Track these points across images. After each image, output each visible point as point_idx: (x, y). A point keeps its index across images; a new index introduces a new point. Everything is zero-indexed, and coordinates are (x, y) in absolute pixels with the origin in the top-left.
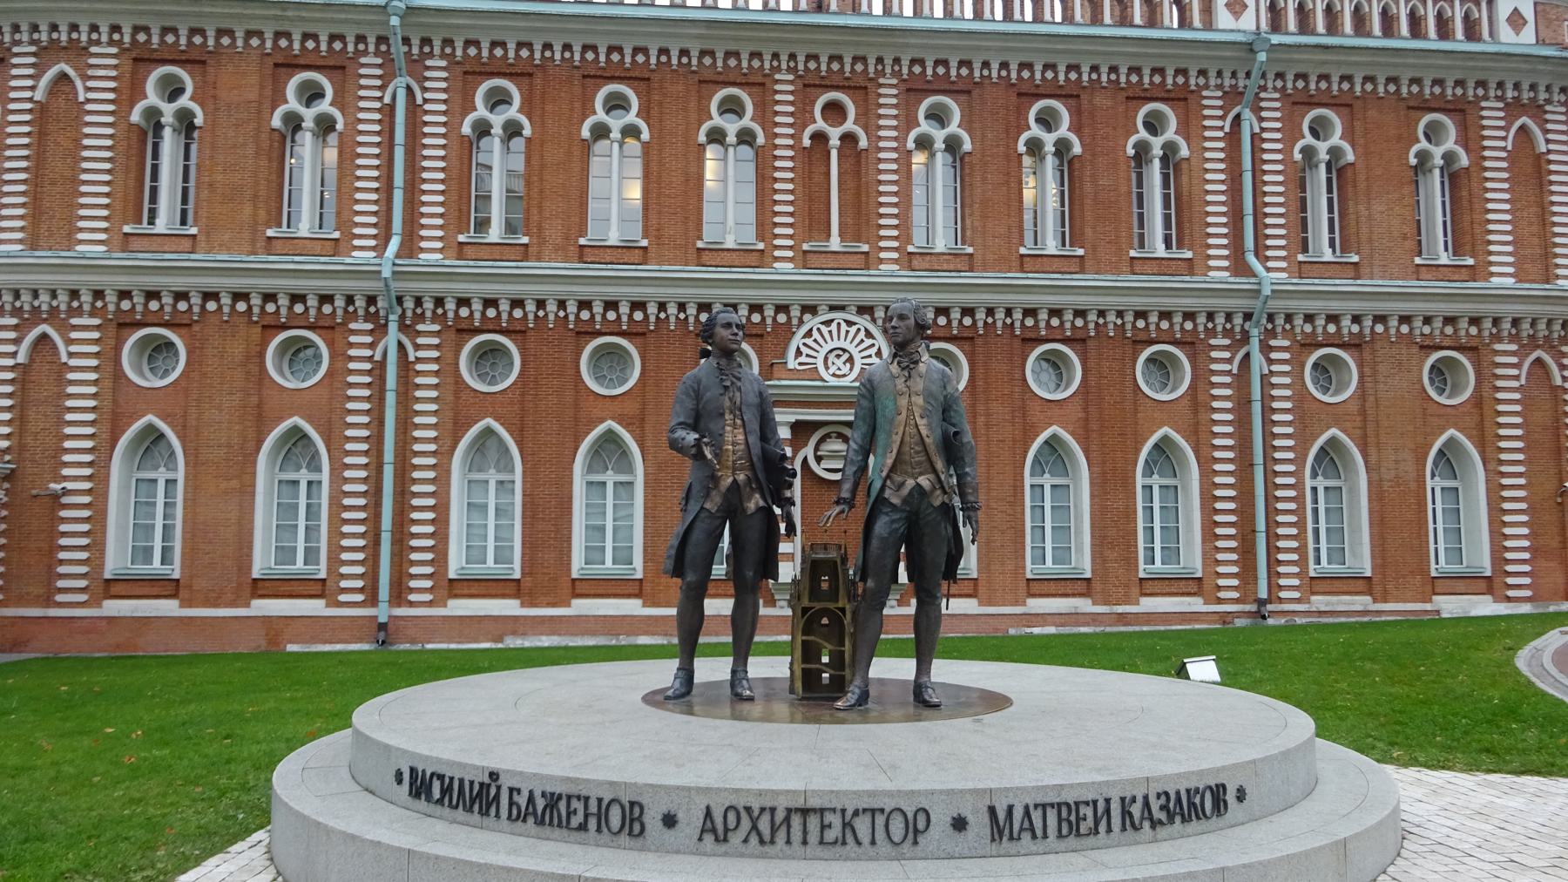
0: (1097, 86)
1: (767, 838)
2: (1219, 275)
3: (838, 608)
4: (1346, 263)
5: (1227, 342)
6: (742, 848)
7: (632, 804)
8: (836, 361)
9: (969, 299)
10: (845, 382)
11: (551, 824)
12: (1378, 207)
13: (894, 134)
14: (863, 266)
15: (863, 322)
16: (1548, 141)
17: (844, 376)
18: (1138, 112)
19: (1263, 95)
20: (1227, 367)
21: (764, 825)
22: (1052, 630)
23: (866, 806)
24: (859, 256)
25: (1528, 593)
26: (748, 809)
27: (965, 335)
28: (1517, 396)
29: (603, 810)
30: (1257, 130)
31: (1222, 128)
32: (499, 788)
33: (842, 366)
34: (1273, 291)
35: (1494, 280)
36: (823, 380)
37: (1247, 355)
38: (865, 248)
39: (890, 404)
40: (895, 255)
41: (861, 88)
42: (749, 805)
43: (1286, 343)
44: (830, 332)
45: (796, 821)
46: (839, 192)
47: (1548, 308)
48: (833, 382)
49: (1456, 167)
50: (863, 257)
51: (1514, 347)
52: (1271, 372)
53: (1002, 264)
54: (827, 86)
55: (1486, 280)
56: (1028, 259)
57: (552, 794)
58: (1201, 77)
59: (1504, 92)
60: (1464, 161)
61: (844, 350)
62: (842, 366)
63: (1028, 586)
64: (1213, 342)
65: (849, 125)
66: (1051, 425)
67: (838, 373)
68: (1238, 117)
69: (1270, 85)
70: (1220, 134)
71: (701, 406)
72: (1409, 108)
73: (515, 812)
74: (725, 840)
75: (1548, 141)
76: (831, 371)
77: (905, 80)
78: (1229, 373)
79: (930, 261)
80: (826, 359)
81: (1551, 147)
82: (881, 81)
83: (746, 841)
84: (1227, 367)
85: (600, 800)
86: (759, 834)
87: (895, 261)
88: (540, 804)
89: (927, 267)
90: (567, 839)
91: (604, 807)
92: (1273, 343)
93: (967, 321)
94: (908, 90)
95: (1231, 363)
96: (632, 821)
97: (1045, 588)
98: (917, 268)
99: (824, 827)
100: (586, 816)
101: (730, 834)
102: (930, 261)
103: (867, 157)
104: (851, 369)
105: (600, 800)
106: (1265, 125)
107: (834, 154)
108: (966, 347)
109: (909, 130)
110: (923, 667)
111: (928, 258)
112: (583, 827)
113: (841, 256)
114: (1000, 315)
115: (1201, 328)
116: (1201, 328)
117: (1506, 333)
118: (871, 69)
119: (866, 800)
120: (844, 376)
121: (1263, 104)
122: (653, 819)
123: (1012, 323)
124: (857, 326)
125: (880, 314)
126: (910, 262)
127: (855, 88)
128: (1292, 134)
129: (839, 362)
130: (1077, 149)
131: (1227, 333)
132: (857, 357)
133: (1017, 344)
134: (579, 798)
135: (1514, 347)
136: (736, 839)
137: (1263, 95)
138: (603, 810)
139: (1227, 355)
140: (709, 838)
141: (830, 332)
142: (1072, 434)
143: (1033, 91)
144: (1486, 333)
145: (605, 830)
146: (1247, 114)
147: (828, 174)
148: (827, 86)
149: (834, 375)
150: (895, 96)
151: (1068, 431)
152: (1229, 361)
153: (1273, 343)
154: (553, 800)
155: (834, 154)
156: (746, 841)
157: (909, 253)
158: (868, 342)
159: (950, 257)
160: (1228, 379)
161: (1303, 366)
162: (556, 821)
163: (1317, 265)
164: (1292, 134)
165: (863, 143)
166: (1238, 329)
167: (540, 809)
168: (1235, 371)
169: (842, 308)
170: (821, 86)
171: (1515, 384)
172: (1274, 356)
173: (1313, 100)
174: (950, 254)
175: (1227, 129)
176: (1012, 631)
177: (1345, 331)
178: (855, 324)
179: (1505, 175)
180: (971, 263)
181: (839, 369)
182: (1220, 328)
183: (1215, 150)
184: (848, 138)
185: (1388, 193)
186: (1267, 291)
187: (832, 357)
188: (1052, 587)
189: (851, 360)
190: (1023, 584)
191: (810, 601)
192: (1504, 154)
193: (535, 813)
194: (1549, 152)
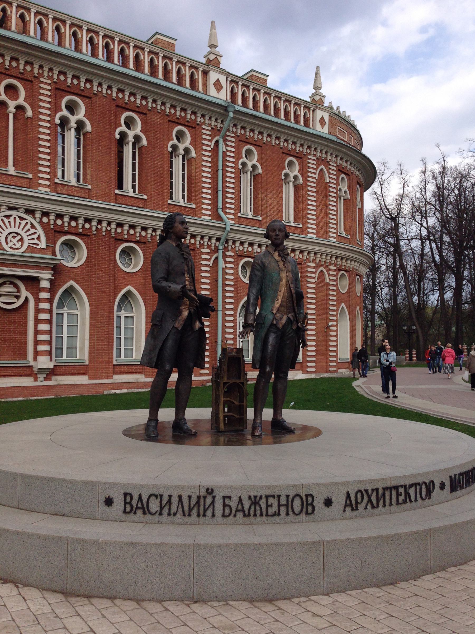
0: (156, 111)
1: (375, 505)
2: (206, 218)
3: (241, 383)
4: (257, 220)
5: (208, 251)
6: (364, 512)
7: (307, 496)
8: (12, 239)
9: (90, 213)
10: (19, 252)
11: (255, 515)
12: (270, 196)
13: (48, 112)
14: (28, 186)
15: (29, 218)
16: (330, 178)
17: (17, 249)
18: (174, 129)
19: (228, 133)
20: (207, 263)
21: (374, 499)
22: (125, 391)
23: (411, 482)
24: (26, 180)
25: (314, 370)
26: (366, 491)
27: (86, 233)
28: (314, 286)
29: (290, 503)
30: (225, 150)
31: (210, 146)
32: (214, 498)
33: (16, 243)
34: (231, 229)
35: (309, 235)
36: (5, 250)
37: (217, 258)
38: (30, 176)
39: (276, 275)
40: (48, 183)
41: (29, 81)
42: (366, 488)
43: (232, 254)
44: (9, 222)
45: (387, 493)
46: (14, 140)
47: (327, 249)
48: (11, 251)
49: (297, 183)
50: (28, 180)
51: (314, 265)
52: (225, 266)
53: (106, 197)
54: (8, 75)
55: (306, 234)
56: (119, 197)
57: (255, 497)
58: (202, 118)
59: (317, 152)
60: (301, 181)
61: (18, 234)
62: (16, 243)
63: (114, 367)
64: (203, 250)
65: (21, 101)
66: (128, 285)
67: (14, 246)
68: (217, 142)
69: (231, 129)
70: (209, 149)
71: (170, 268)
72: (283, 153)
73: (227, 511)
74: (357, 509)
75: (330, 178)
76: (10, 244)
77: (55, 82)
78: (208, 266)
79: (67, 190)
80: (6, 238)
81: (331, 180)
82: (42, 79)
83: (366, 508)
84: (207, 263)
85: (288, 496)
86: (372, 504)
87: (48, 186)
88: (247, 504)
89: (66, 192)
90: (266, 522)
91: (290, 500)
92: (227, 253)
93: (87, 226)
94: (57, 89)
95: (210, 261)
96: (307, 504)
97: (122, 369)
98: (60, 192)
99: (398, 495)
100: (279, 505)
101: (358, 505)
102: (67, 190)
103: (31, 123)
104: (22, 246)
105: (288, 496)
106: (228, 148)
107: (11, 117)
108: (86, 240)
109: (56, 112)
110: (180, 411)
111: (66, 187)
112: (278, 514)
113: (15, 178)
114: (104, 225)
115: (198, 243)
116: (198, 243)
117: (312, 259)
118: (36, 71)
119: (412, 479)
120: (17, 249)
121: (228, 138)
122: (319, 503)
123: (110, 230)
124: (26, 221)
125: (38, 215)
126: (55, 188)
127: (26, 80)
128: (238, 157)
129: (15, 241)
130: (144, 142)
131: (209, 246)
132: (26, 239)
133: (112, 241)
134: (273, 496)
135: (314, 265)
136: (361, 507)
137: (228, 133)
138: (290, 503)
139: (208, 257)
140: (348, 509)
141: (9, 222)
142: (138, 290)
143: (124, 105)
144: (305, 258)
145: (291, 513)
146: (221, 141)
147: (7, 127)
148: (8, 75)
149: (11, 248)
150: (49, 90)
151: (136, 289)
152: (209, 260)
153: (227, 253)
154: (255, 501)
155: (11, 117)
156: (366, 508)
157: (56, 183)
158: (32, 231)
159: (79, 189)
160: (208, 269)
161: (238, 265)
162: (258, 512)
163: (245, 219)
164: (238, 157)
165: (29, 113)
166: (213, 245)
167: (246, 507)
168: (211, 265)
169: (16, 209)
170: (4, 74)
171: (313, 281)
172: (228, 259)
173: (248, 141)
174: (78, 187)
175: (212, 147)
176: (105, 392)
177: (255, 251)
178: (25, 219)
179: (315, 190)
180: (89, 194)
181: (14, 244)
182: (206, 244)
183: (207, 157)
184: (19, 108)
185: (274, 190)
186: (228, 229)
187: (10, 237)
188: (126, 369)
189: (21, 240)
190: (111, 368)
191: (227, 379)
192: (315, 181)
193: (243, 510)
194: (330, 182)
